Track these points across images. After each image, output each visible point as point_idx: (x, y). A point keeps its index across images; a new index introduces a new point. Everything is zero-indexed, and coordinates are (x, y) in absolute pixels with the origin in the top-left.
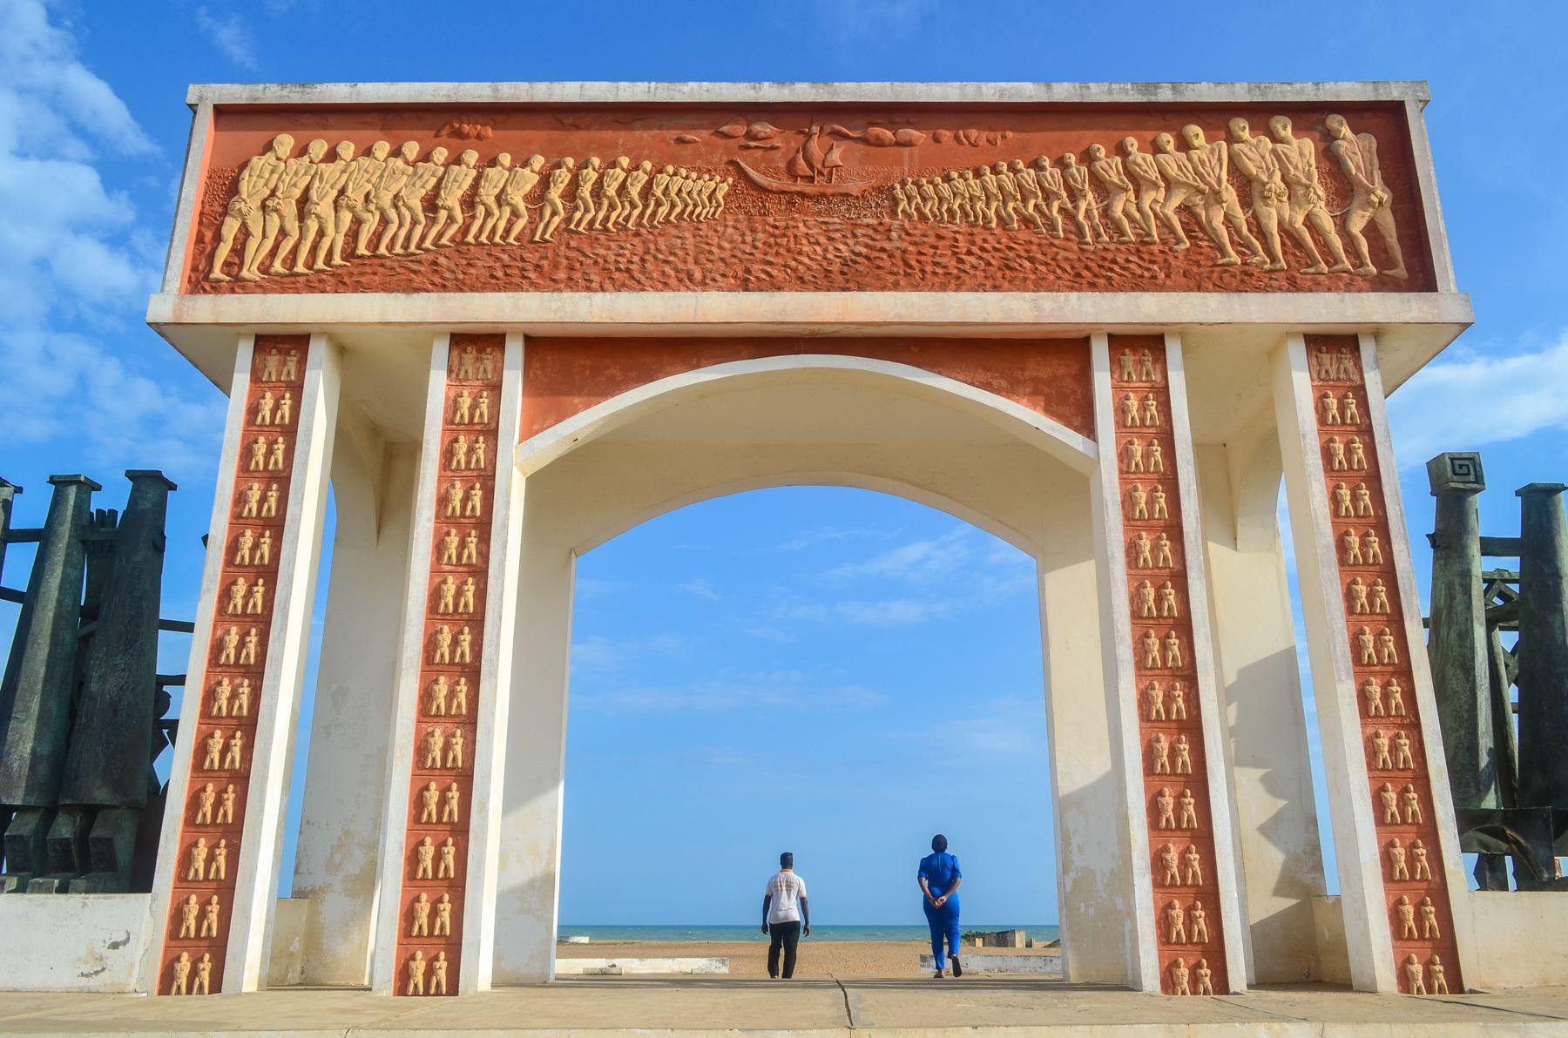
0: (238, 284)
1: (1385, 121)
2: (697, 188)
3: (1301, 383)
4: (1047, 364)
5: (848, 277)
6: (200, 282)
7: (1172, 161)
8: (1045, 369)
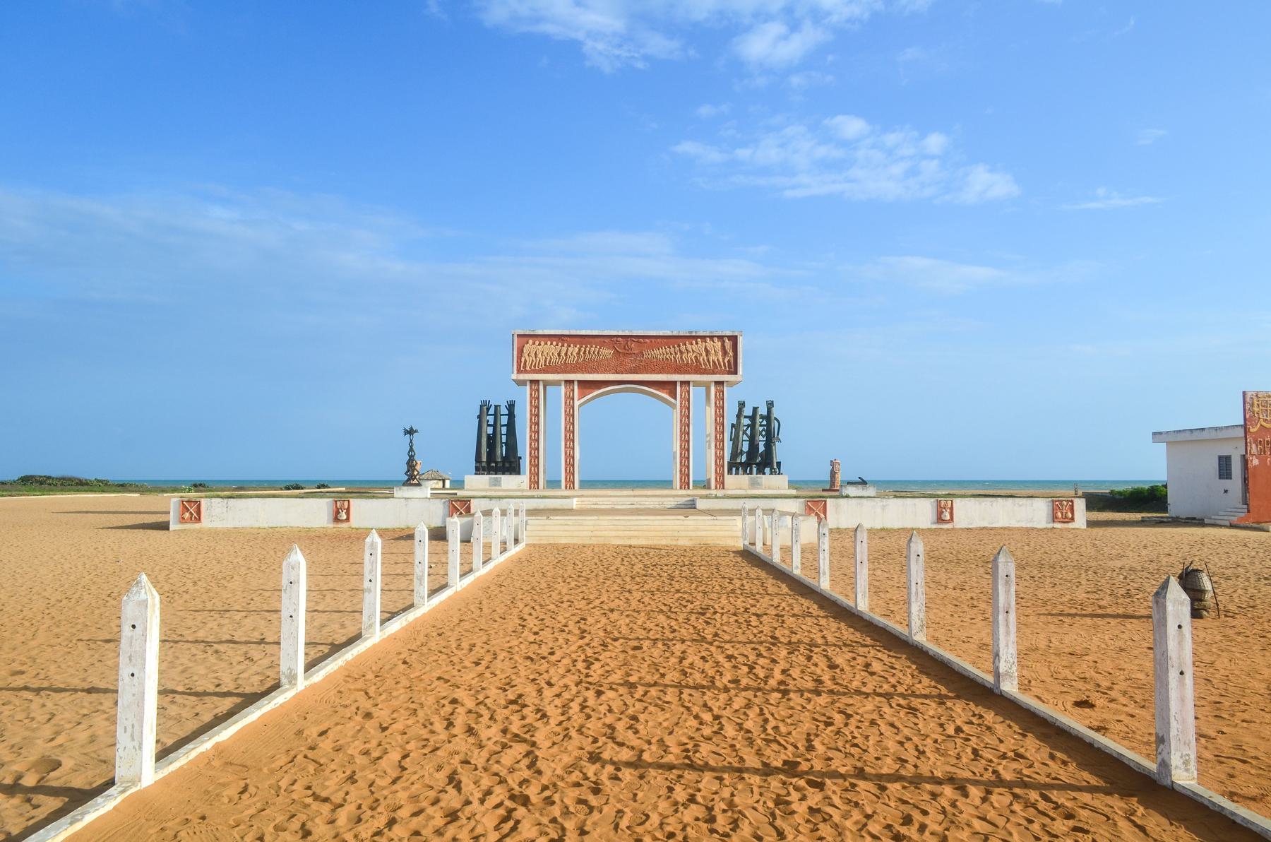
0: (526, 372)
1: (734, 339)
2: (607, 352)
3: (713, 389)
4: (670, 386)
5: (635, 371)
6: (519, 371)
7: (694, 347)
8: (671, 387)
